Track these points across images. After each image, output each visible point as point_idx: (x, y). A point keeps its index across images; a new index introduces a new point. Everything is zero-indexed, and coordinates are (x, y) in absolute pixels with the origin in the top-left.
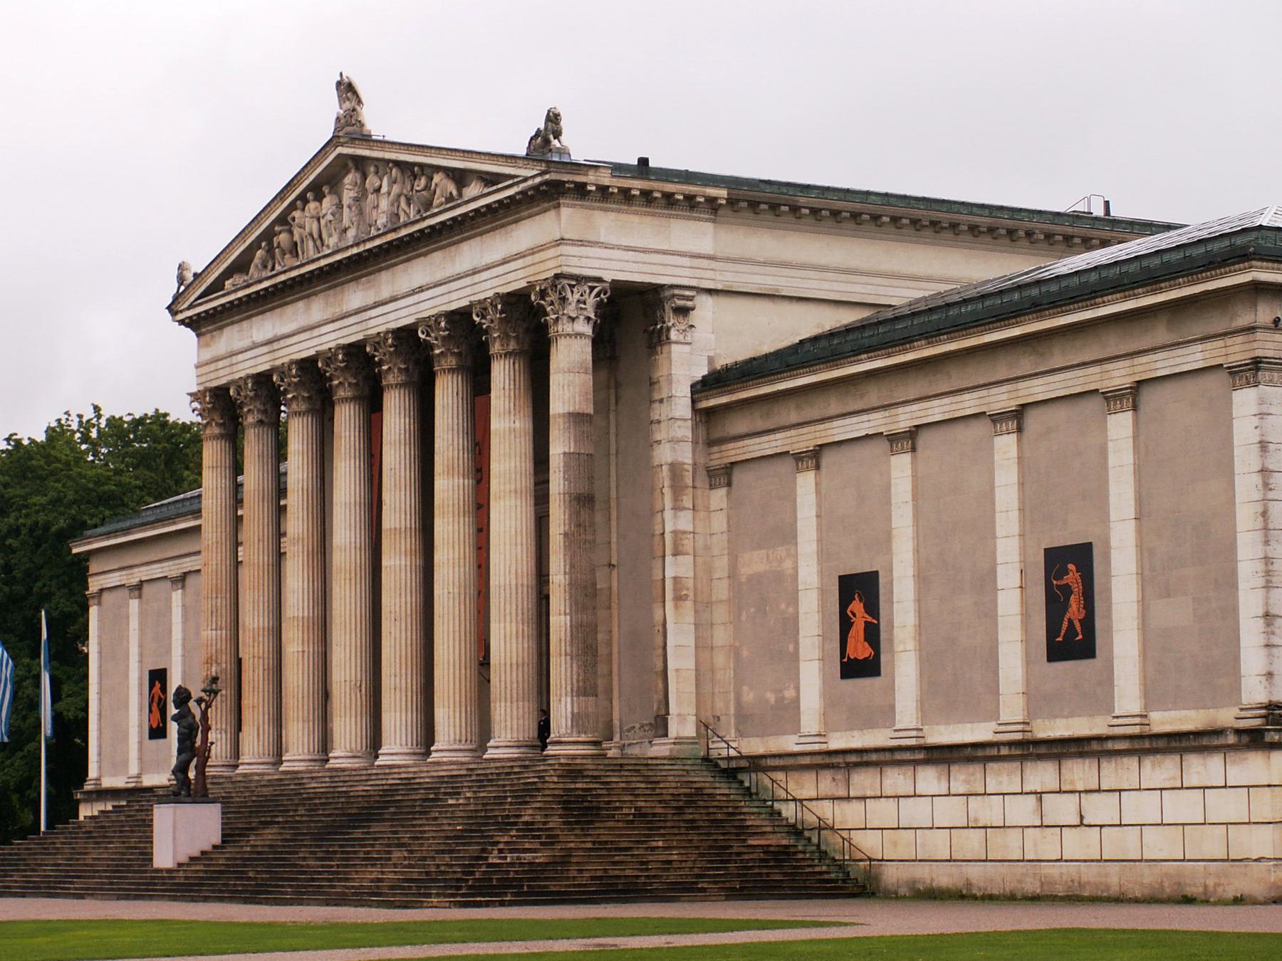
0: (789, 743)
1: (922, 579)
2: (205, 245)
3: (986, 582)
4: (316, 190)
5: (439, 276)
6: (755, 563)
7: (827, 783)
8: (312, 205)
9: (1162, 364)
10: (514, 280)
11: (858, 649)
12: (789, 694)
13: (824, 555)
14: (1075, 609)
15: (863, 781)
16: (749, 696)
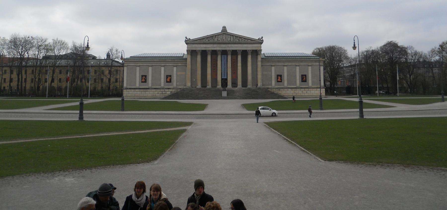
0: (270, 87)
1: (287, 76)
2: (193, 37)
4: (218, 35)
7: (277, 90)
8: (217, 37)
9: (314, 64)
11: (279, 80)
12: (270, 83)
13: (275, 73)
14: (304, 79)
15: (281, 90)
16: (264, 83)
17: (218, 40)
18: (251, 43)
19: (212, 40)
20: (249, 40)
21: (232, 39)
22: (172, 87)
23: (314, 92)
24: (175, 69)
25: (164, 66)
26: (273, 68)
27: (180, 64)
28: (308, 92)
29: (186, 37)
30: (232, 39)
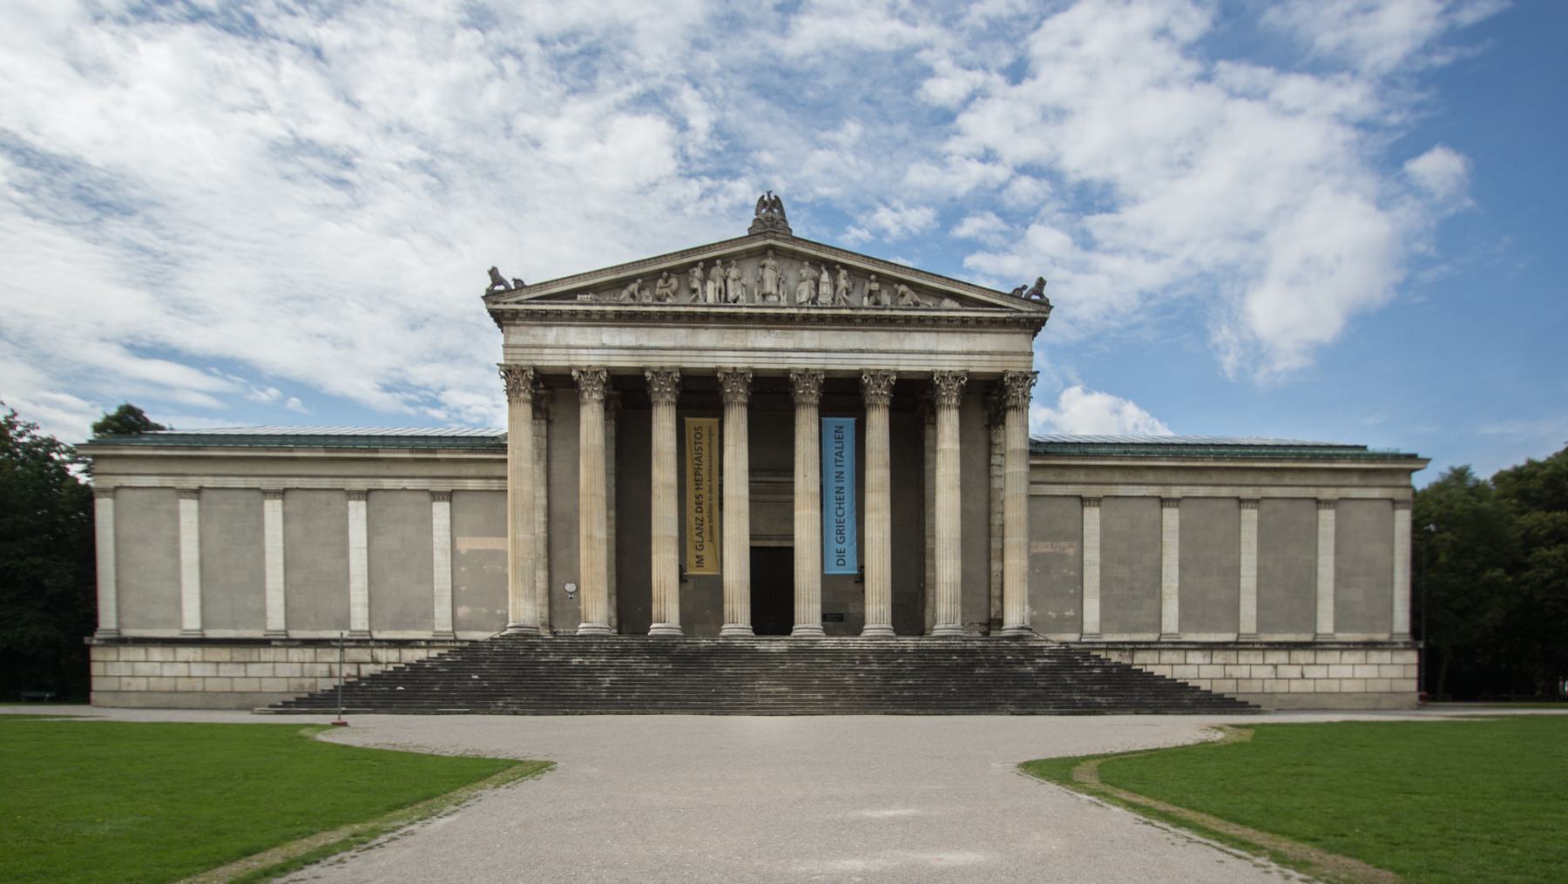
3: (1236, 571)
5: (882, 347)
6: (1043, 548)
10: (981, 366)
17: (722, 293)
18: (963, 325)
19: (686, 298)
20: (947, 303)
21: (826, 289)
22: (426, 635)
23: (1346, 671)
24: (441, 510)
25: (366, 494)
26: (1092, 516)
27: (471, 484)
28: (1311, 672)
29: (493, 273)
30: (826, 289)
